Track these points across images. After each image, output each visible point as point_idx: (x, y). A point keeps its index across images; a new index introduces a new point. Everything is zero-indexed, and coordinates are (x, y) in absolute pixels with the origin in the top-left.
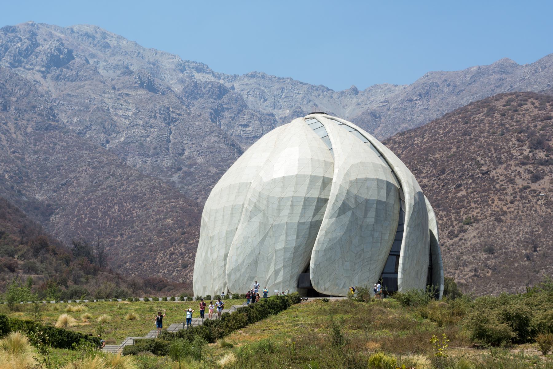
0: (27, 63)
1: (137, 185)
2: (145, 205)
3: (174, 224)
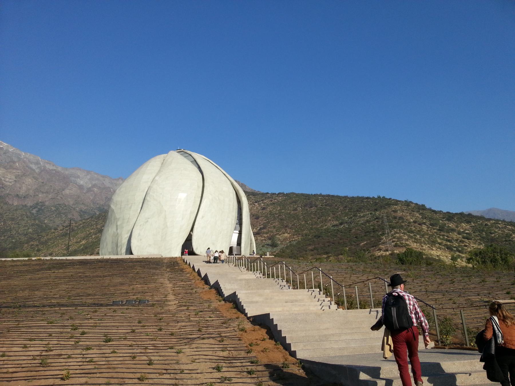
2: (18, 222)
3: (33, 232)
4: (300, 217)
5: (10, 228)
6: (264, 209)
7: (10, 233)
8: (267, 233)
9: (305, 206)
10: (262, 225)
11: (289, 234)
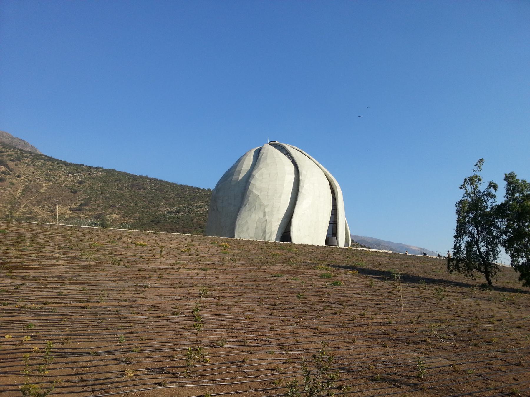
4: (128, 198)
6: (81, 182)
8: (90, 211)
9: (132, 186)
10: (82, 200)
11: (117, 215)
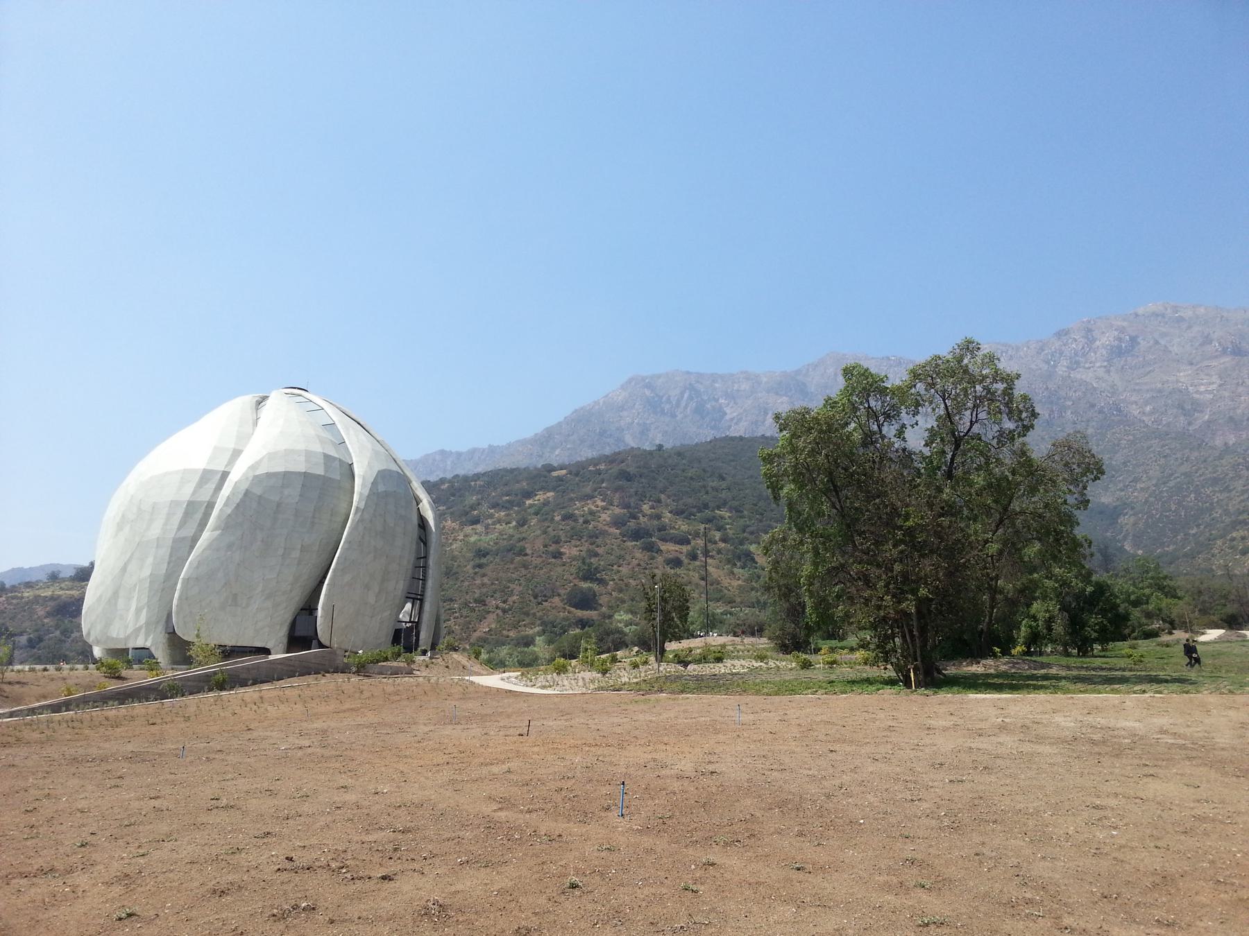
0: (1086, 362)
1: (1217, 466)
5: (1212, 504)
7: (1210, 515)
